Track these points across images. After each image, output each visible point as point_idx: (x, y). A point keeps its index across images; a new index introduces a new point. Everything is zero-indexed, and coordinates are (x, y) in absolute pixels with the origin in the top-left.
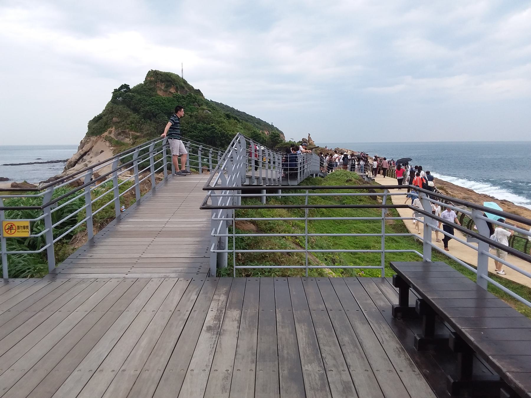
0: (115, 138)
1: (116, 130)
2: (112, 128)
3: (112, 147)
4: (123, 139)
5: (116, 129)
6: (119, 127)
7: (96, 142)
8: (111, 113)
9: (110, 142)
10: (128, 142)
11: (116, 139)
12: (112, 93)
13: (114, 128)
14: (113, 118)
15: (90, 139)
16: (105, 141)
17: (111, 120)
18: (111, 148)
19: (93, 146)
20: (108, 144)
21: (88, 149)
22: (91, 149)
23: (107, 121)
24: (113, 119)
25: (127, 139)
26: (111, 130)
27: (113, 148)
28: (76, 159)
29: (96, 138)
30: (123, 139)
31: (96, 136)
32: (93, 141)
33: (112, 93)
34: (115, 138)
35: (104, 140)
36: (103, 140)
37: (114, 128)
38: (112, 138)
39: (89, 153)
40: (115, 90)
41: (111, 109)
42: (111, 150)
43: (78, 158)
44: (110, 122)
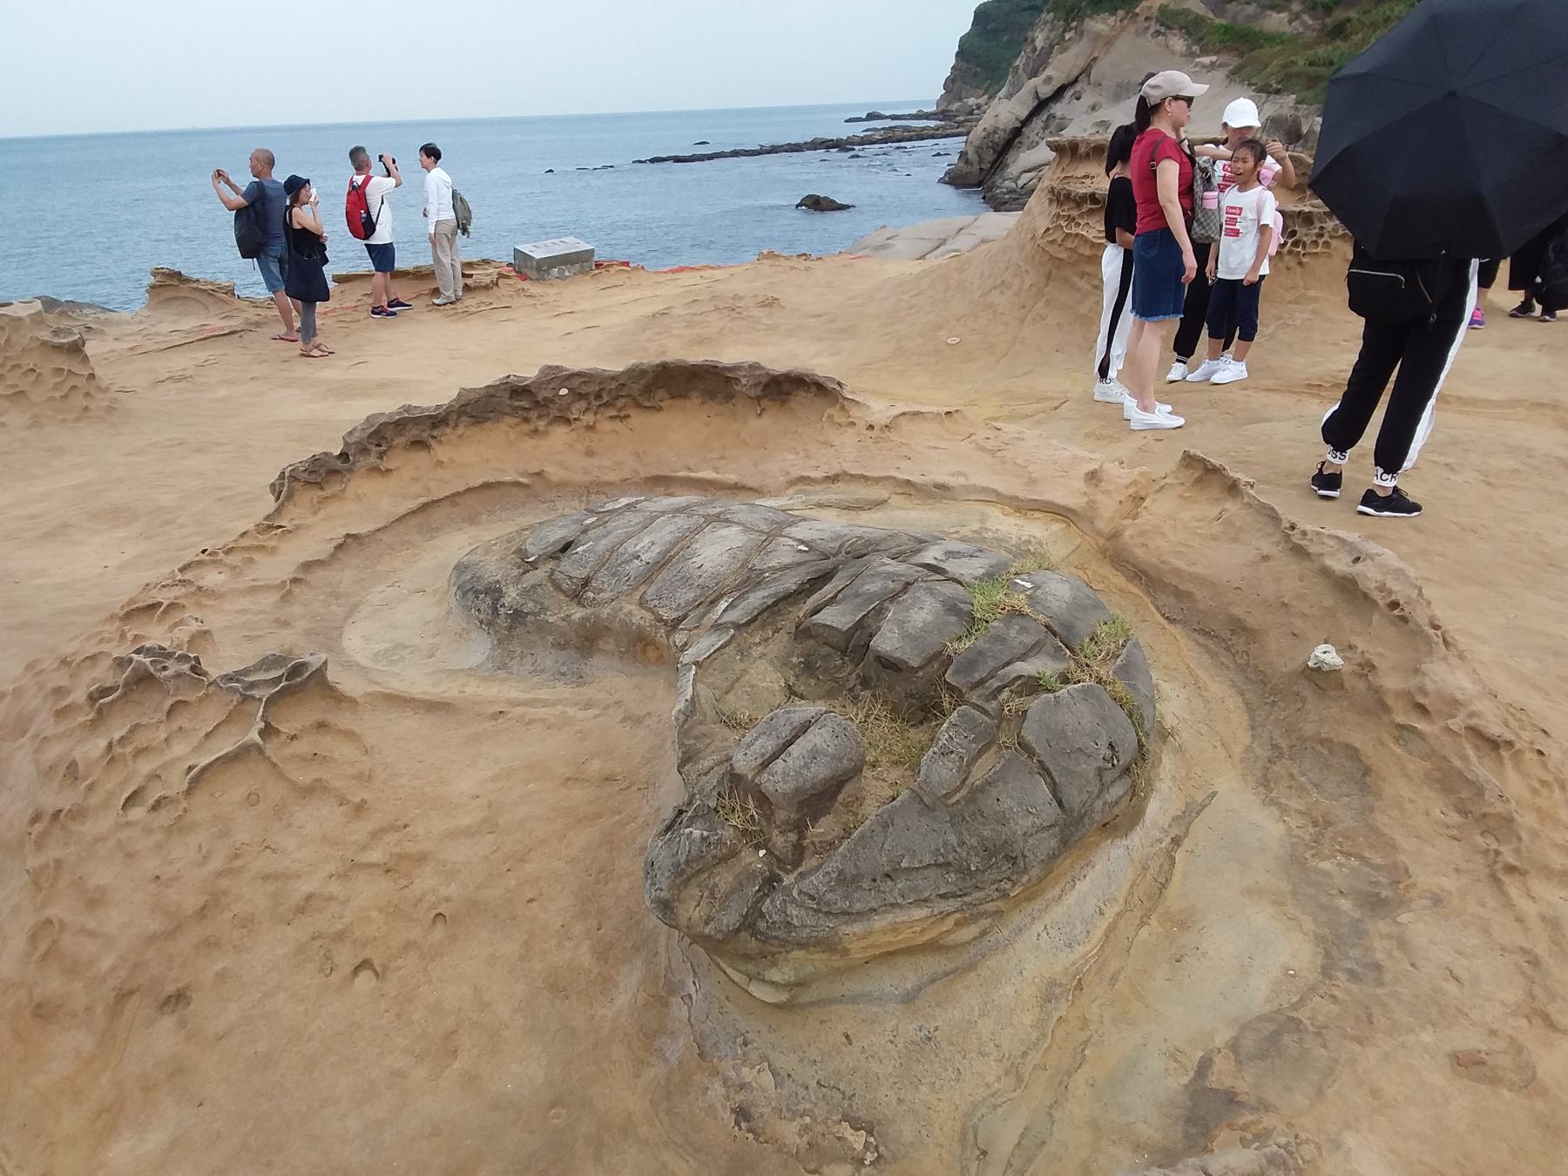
0: (1211, 15)
3: (1204, 52)
4: (1255, 17)
7: (1109, 42)
9: (1189, 33)
10: (1288, 29)
11: (1217, 21)
15: (1076, 28)
16: (1163, 29)
18: (1206, 60)
19: (1095, 59)
20: (1178, 43)
21: (1075, 73)
22: (1086, 71)
25: (1274, 15)
27: (1214, 58)
28: (1017, 119)
29: (1112, 20)
30: (1255, 17)
31: (1113, 12)
32: (1097, 37)
35: (1154, 27)
36: (1148, 28)
38: (1198, 16)
39: (1078, 87)
42: (1204, 66)
43: (1024, 114)
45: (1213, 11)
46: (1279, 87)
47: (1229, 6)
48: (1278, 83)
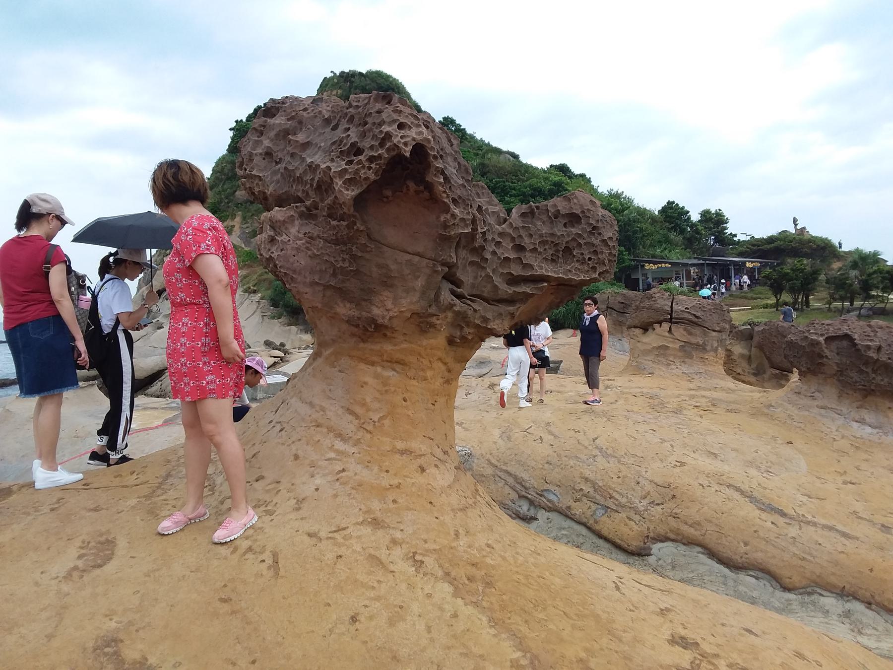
0: (243, 246)
1: (247, 223)
2: (233, 219)
5: (244, 218)
6: (253, 215)
8: (228, 179)
11: (246, 249)
12: (231, 129)
13: (238, 219)
14: (235, 191)
17: (232, 197)
23: (220, 202)
24: (237, 193)
26: (232, 224)
33: (231, 129)
34: (243, 246)
37: (238, 219)
40: (237, 122)
41: (229, 166)
44: (228, 203)
45: (244, 243)
46: (255, 288)
47: (252, 240)
48: (254, 286)
